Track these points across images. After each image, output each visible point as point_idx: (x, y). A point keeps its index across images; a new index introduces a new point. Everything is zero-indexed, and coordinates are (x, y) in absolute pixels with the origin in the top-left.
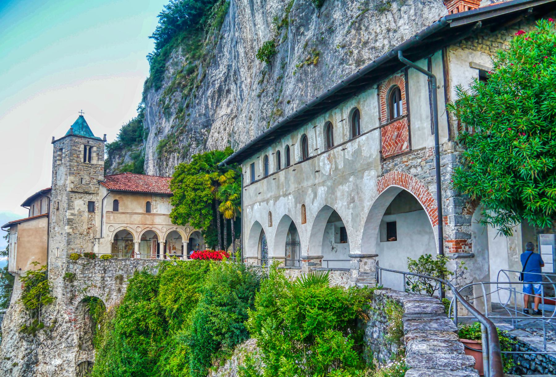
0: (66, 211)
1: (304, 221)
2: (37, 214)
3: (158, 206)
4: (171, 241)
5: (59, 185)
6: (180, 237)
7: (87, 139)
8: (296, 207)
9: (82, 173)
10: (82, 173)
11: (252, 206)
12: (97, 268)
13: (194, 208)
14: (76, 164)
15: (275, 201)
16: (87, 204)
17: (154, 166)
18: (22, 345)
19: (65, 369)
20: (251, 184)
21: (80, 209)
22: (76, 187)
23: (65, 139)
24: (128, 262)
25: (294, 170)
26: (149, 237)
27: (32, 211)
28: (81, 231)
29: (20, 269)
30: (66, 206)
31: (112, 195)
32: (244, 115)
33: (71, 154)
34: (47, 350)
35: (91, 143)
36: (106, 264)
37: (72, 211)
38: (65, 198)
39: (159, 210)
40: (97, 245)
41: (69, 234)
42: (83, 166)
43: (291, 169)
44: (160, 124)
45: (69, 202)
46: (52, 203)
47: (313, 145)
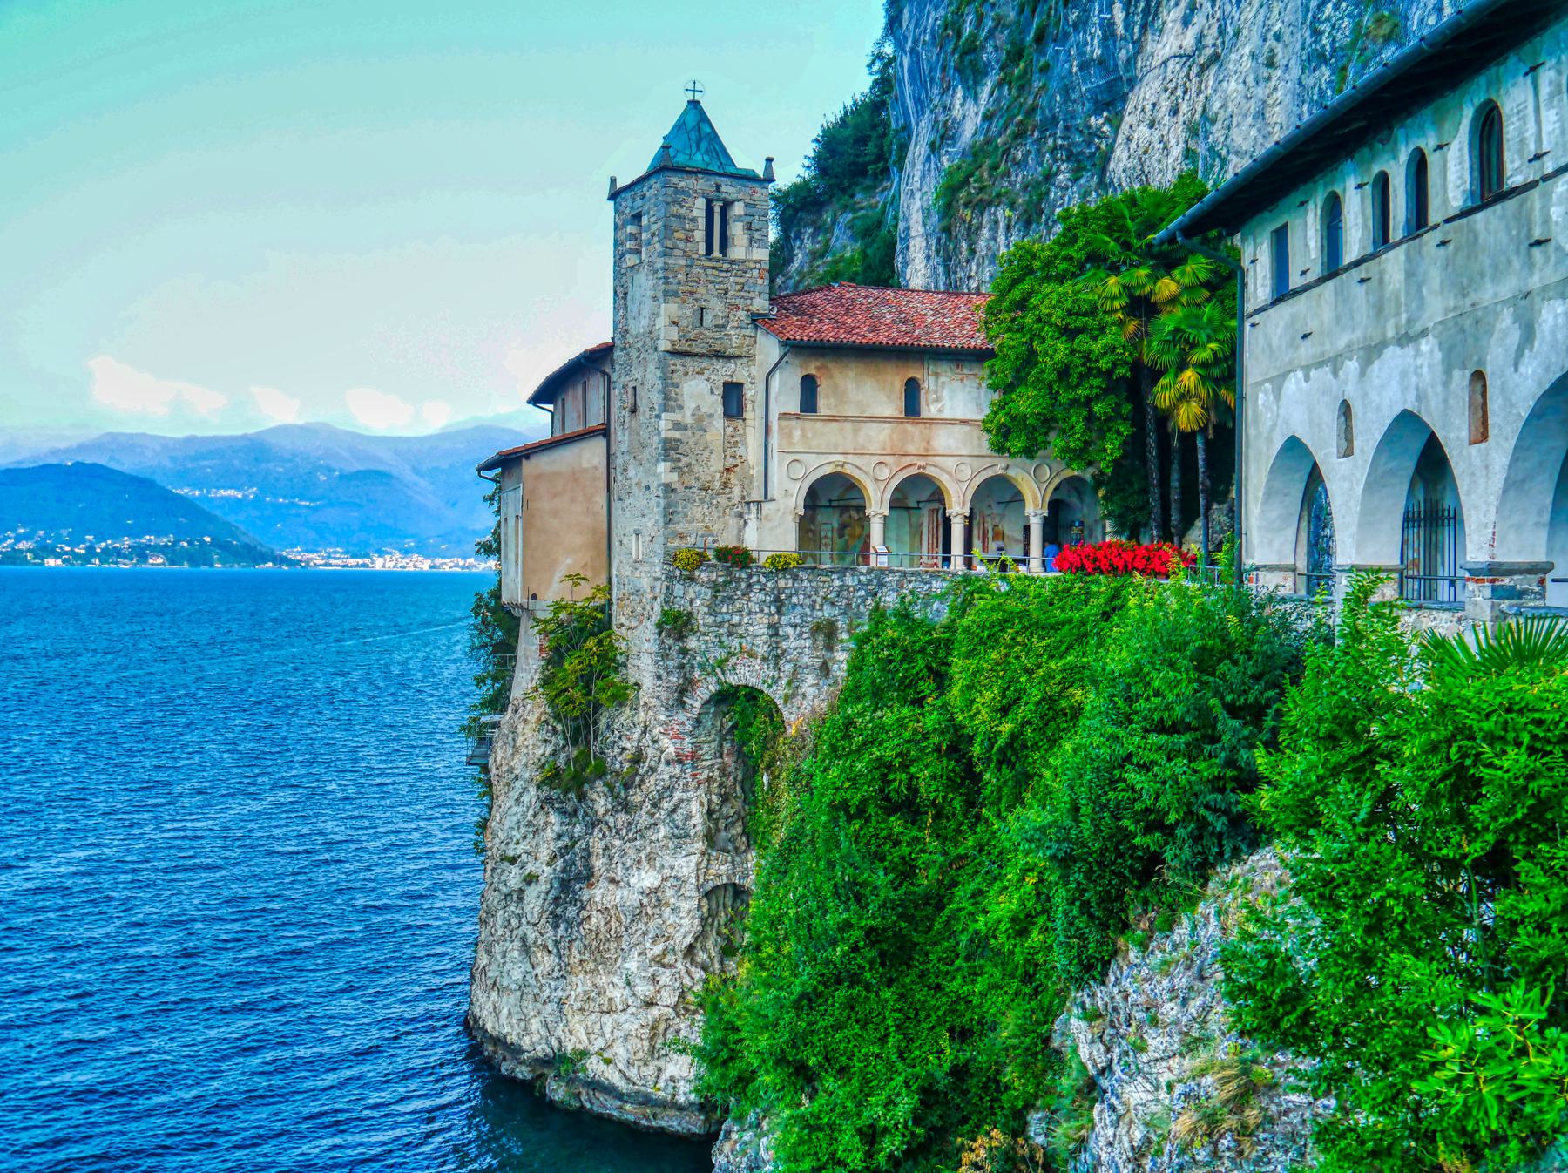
0: (658, 416)
1: (1481, 433)
2: (573, 427)
3: (946, 393)
4: (988, 512)
5: (633, 331)
6: (1017, 499)
7: (714, 180)
8: (1446, 384)
9: (701, 290)
10: (701, 290)
11: (1278, 382)
12: (756, 596)
13: (1065, 397)
14: (682, 262)
15: (1366, 363)
16: (719, 391)
17: (928, 258)
18: (546, 823)
19: (667, 904)
20: (1276, 302)
21: (698, 408)
22: (684, 337)
23: (647, 184)
24: (850, 580)
25: (1443, 243)
26: (918, 496)
27: (559, 419)
28: (704, 478)
29: (534, 597)
30: (657, 398)
31: (797, 361)
32: (1247, 51)
33: (668, 231)
34: (617, 842)
35: (728, 189)
36: (782, 583)
37: (676, 416)
38: (653, 374)
39: (948, 405)
40: (753, 524)
41: (669, 489)
42: (704, 268)
43: (1431, 238)
44: (947, 109)
45: (665, 386)
46: (616, 392)
47: (1522, 141)
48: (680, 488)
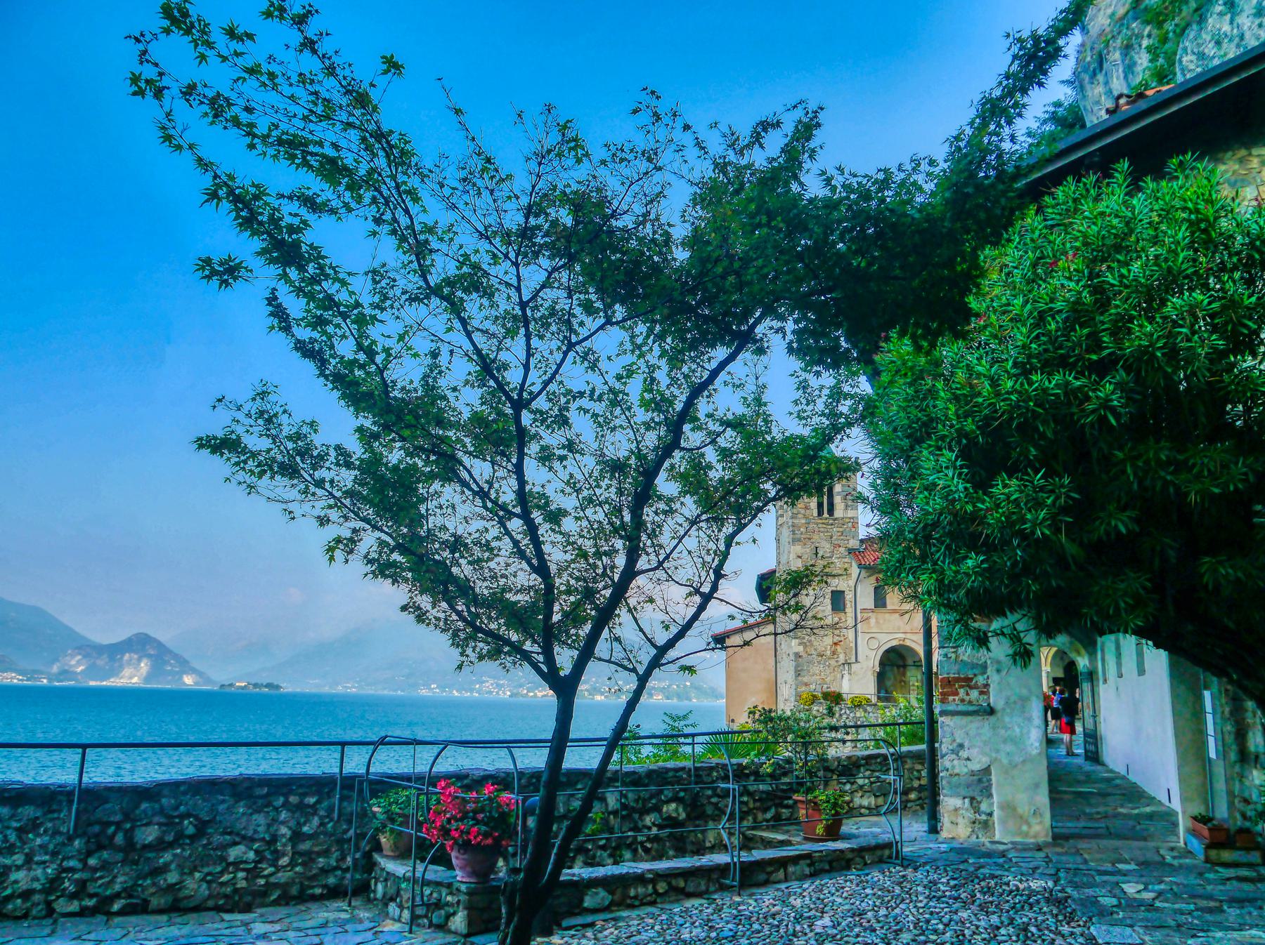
9: (816, 537)
10: (816, 537)
28: (820, 649)
40: (846, 677)
41: (798, 656)
48: (804, 655)
